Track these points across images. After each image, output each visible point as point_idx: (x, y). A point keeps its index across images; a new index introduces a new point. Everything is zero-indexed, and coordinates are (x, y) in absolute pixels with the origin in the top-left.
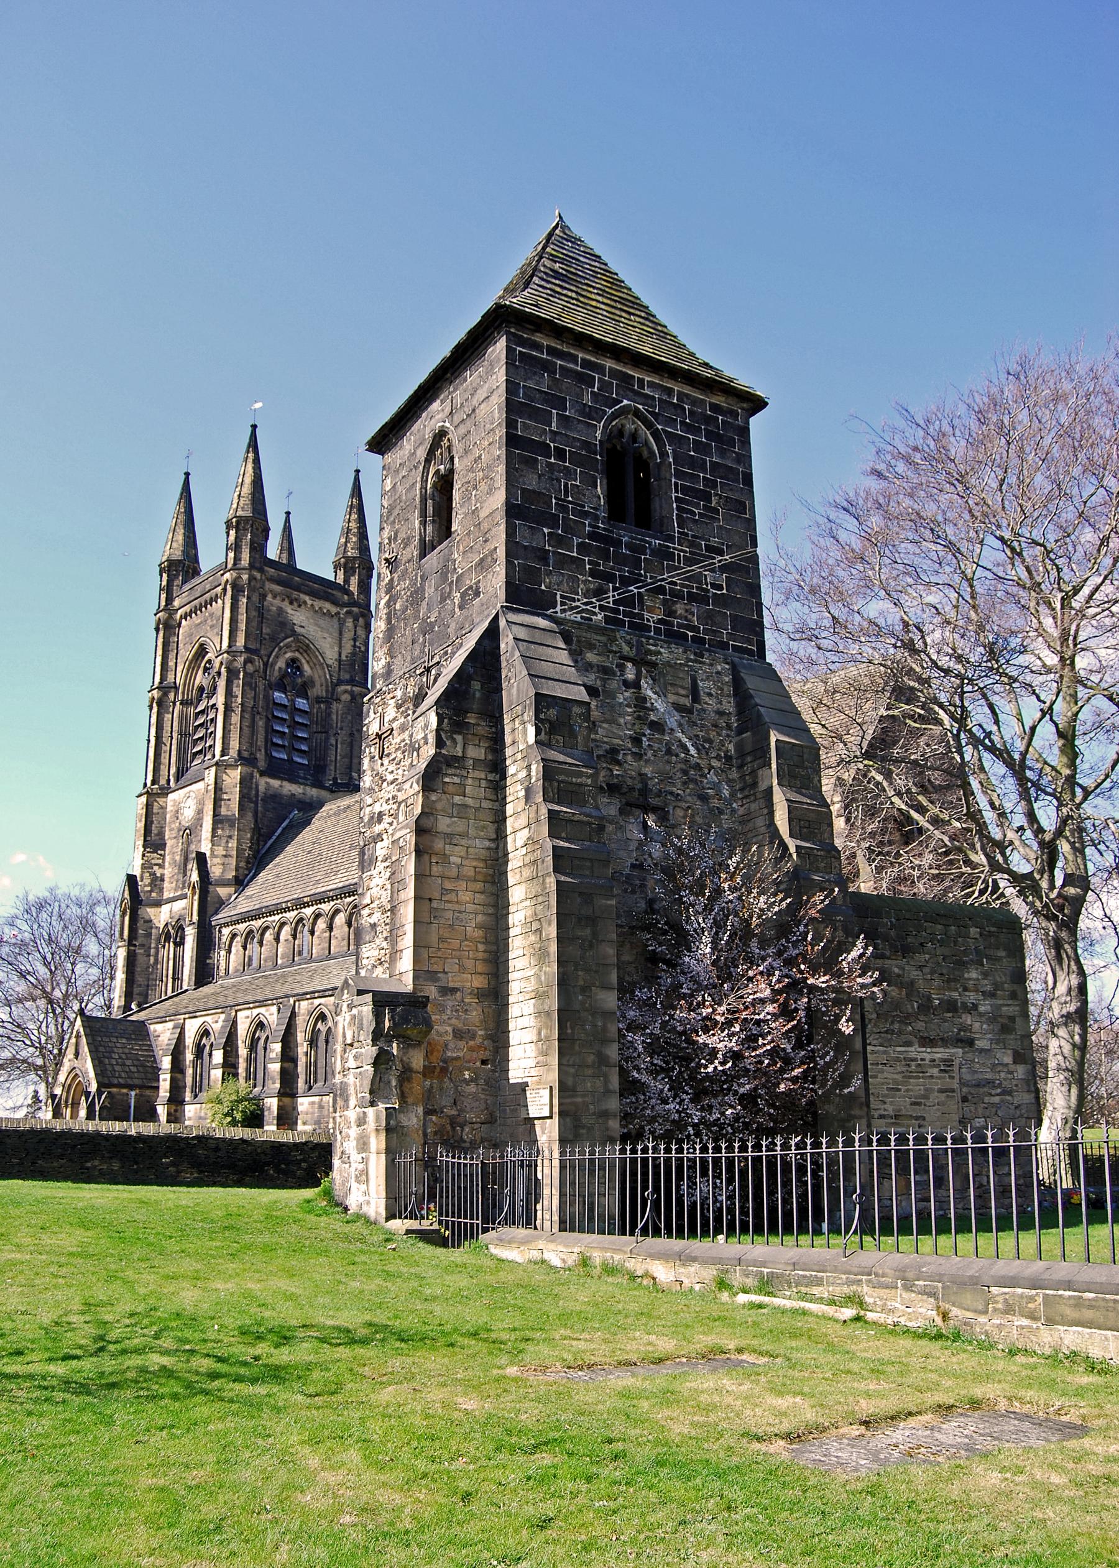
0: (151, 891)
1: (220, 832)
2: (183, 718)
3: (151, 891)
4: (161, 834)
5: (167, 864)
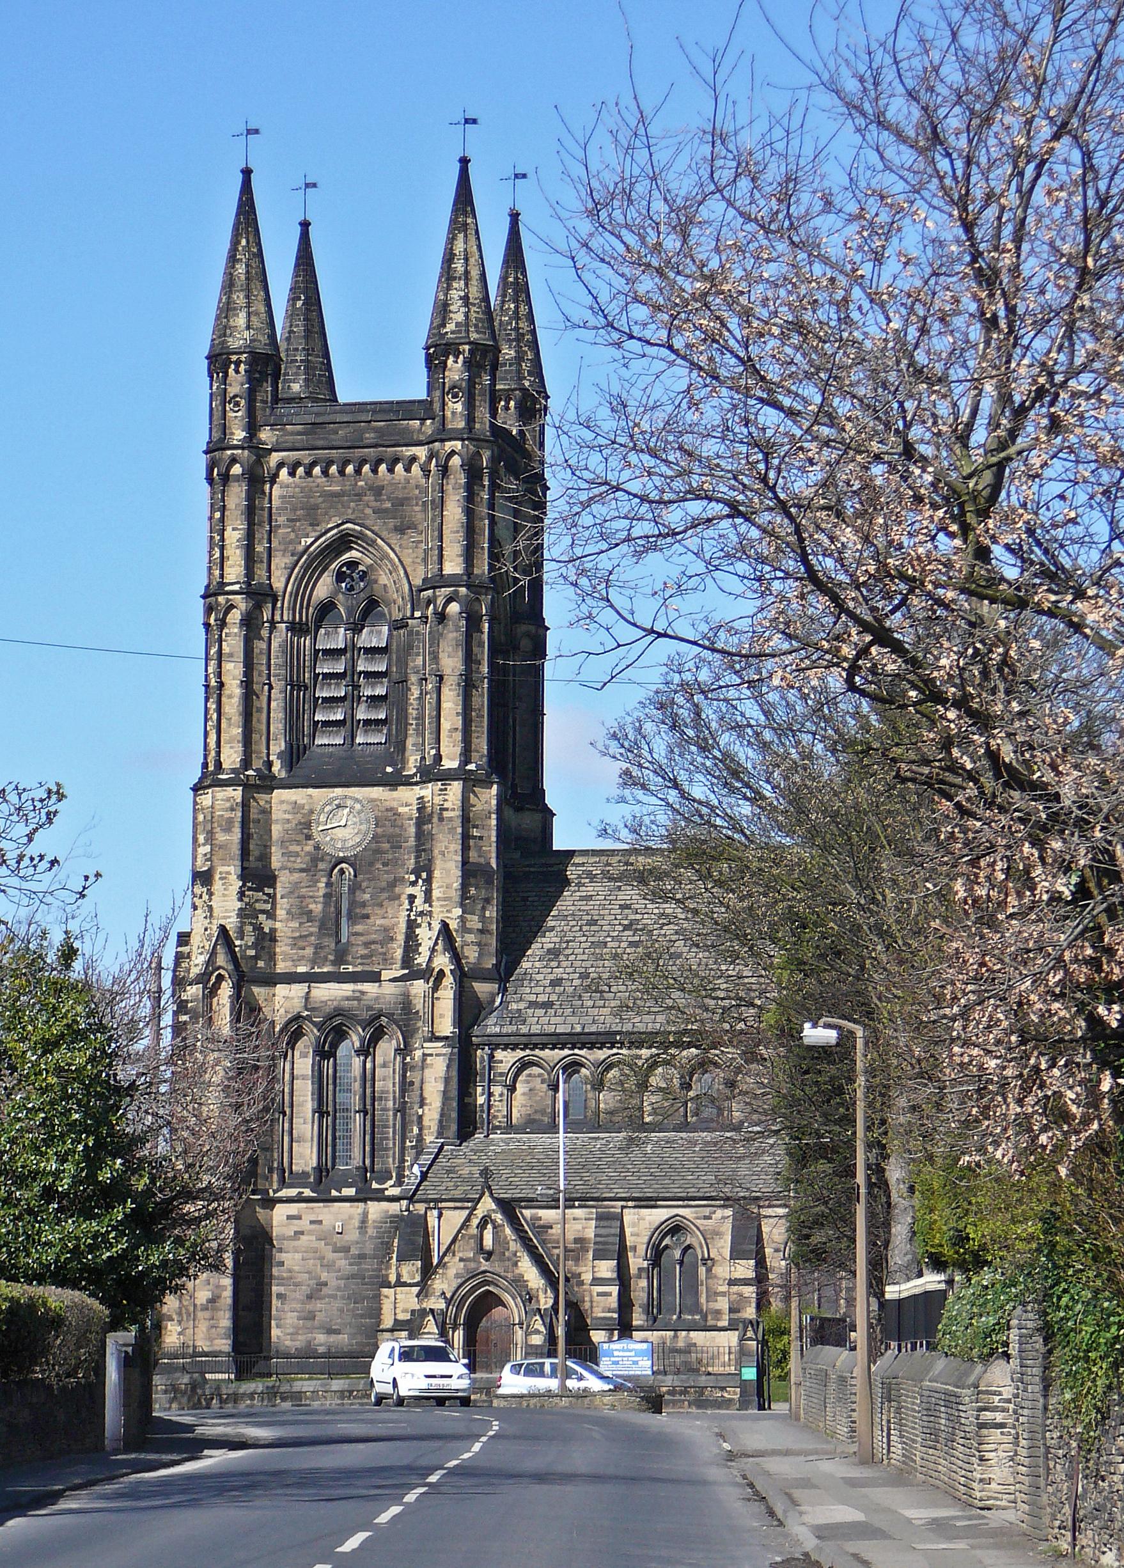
0: (256, 958)
1: (473, 891)
2: (292, 655)
3: (256, 958)
4: (265, 857)
5: (281, 913)
